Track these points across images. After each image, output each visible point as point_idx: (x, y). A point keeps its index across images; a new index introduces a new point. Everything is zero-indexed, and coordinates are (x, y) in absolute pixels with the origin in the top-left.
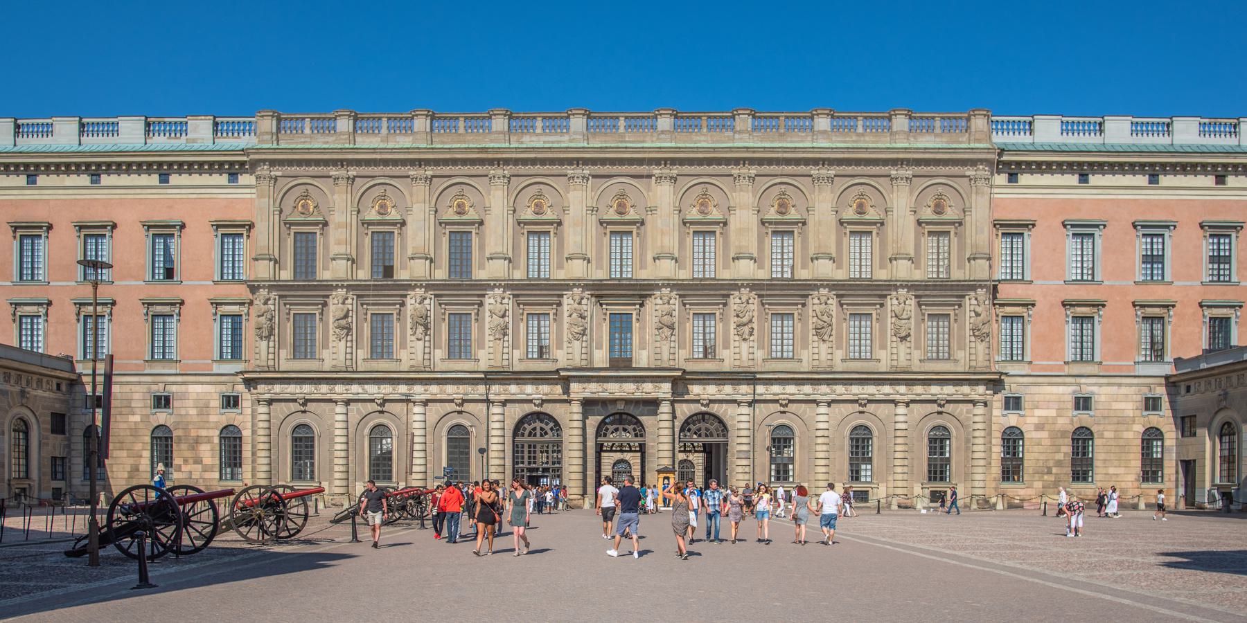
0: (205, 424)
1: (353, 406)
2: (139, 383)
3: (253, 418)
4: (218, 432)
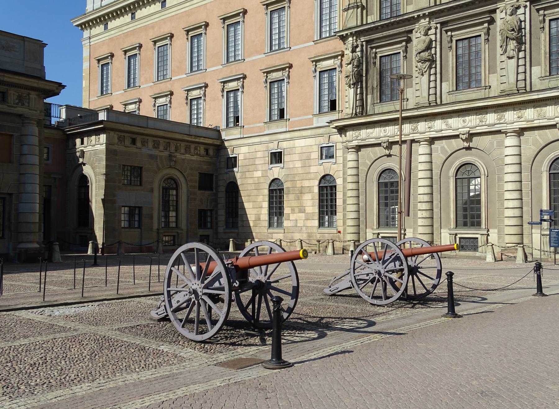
0: (307, 175)
1: (438, 145)
2: (260, 143)
3: (344, 165)
4: (317, 182)
